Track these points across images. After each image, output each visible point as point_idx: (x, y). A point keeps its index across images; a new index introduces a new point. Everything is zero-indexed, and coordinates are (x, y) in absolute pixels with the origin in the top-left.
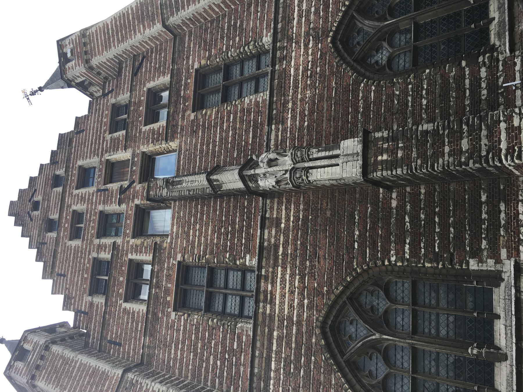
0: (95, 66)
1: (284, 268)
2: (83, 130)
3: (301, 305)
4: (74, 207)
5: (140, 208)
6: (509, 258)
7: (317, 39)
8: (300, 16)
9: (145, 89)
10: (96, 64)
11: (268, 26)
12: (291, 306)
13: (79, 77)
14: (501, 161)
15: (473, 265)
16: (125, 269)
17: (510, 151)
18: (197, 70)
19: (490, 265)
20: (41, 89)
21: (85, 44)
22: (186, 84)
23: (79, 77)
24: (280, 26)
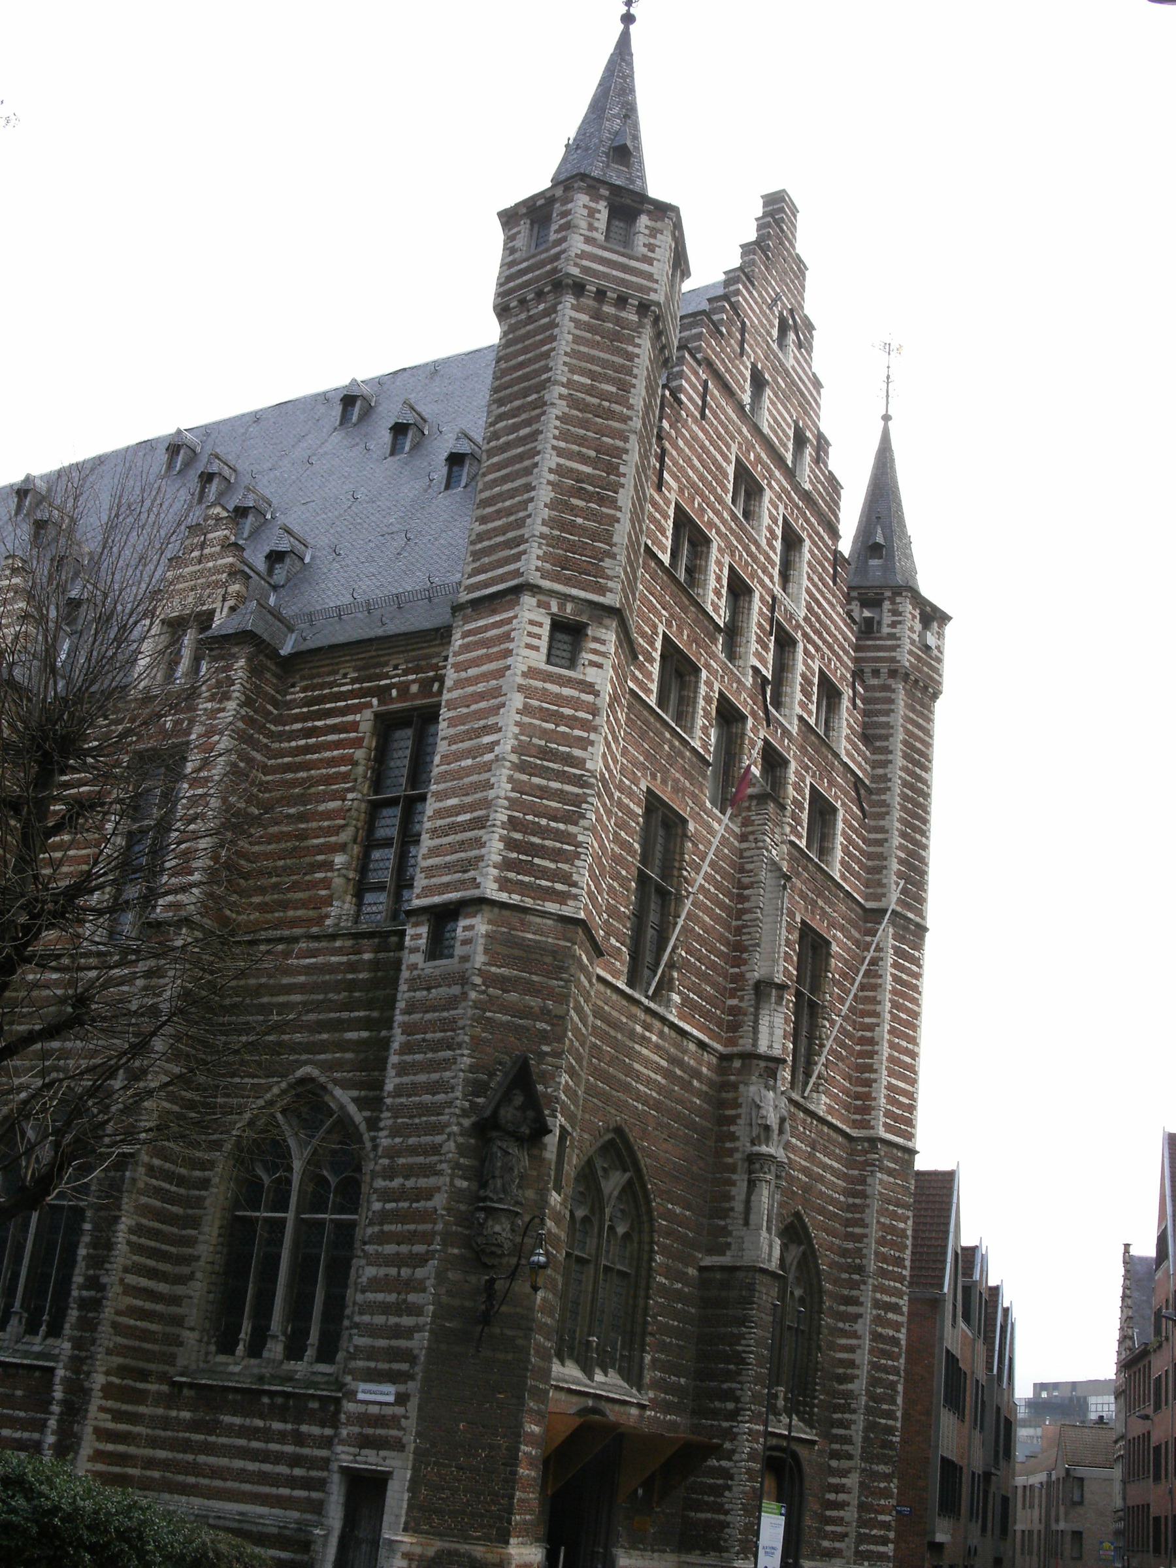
0: (891, 681)
1: (667, 1074)
2: (835, 583)
3: (638, 1097)
4: (768, 495)
5: (737, 721)
6: (650, 1400)
7: (807, 1189)
8: (825, 1167)
9: (838, 805)
10: (893, 691)
11: (830, 1110)
12: (638, 1076)
13: (894, 625)
14: (746, 1422)
15: (648, 1358)
16: (691, 652)
17: (751, 1432)
18: (828, 943)
19: (647, 1379)
20: (886, 418)
21: (926, 688)
22: (824, 913)
23: (894, 625)
24: (826, 1129)
